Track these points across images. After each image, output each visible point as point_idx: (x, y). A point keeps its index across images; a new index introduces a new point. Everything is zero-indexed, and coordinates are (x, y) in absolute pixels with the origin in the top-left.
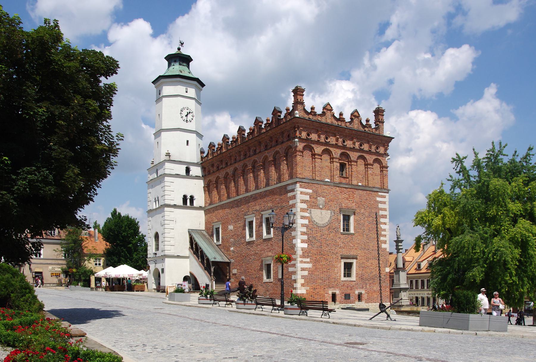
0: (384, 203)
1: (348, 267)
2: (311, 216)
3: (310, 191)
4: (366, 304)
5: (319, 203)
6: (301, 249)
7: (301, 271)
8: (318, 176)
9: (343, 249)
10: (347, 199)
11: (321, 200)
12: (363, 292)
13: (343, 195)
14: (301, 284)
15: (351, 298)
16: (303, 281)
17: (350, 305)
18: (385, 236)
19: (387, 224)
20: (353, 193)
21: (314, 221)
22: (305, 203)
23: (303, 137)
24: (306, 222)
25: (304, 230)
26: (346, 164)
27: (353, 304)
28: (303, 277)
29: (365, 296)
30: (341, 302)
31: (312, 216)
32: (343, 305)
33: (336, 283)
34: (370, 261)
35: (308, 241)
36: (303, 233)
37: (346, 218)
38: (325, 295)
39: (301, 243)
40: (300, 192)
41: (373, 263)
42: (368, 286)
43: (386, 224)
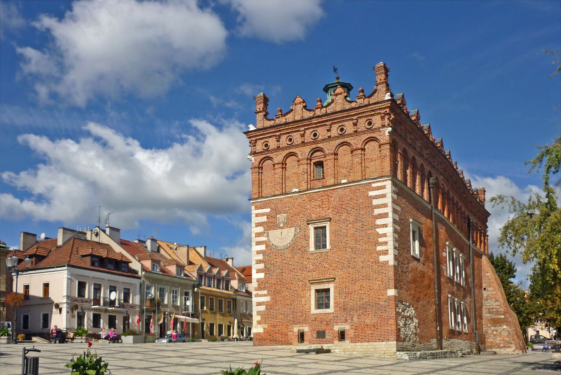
0: (384, 196)
1: (323, 294)
2: (269, 239)
3: (268, 210)
4: (351, 344)
5: (279, 222)
6: (256, 281)
7: (257, 305)
8: (279, 189)
9: (313, 272)
10: (319, 206)
11: (281, 217)
12: (347, 327)
13: (313, 203)
14: (257, 321)
15: (327, 337)
16: (259, 318)
17: (325, 347)
18: (386, 243)
19: (389, 225)
20: (328, 196)
21: (273, 245)
22: (261, 226)
23: (260, 151)
24: (263, 247)
25: (260, 257)
26: (323, 161)
27: (329, 345)
28: (259, 313)
29: (350, 333)
30: (310, 342)
31: (270, 239)
32: (314, 345)
33: (304, 318)
34: (358, 284)
35: (265, 270)
36: (258, 262)
37: (320, 232)
38: (289, 333)
39: (257, 273)
40: (255, 215)
41: (364, 285)
42: (355, 319)
43: (386, 226)
